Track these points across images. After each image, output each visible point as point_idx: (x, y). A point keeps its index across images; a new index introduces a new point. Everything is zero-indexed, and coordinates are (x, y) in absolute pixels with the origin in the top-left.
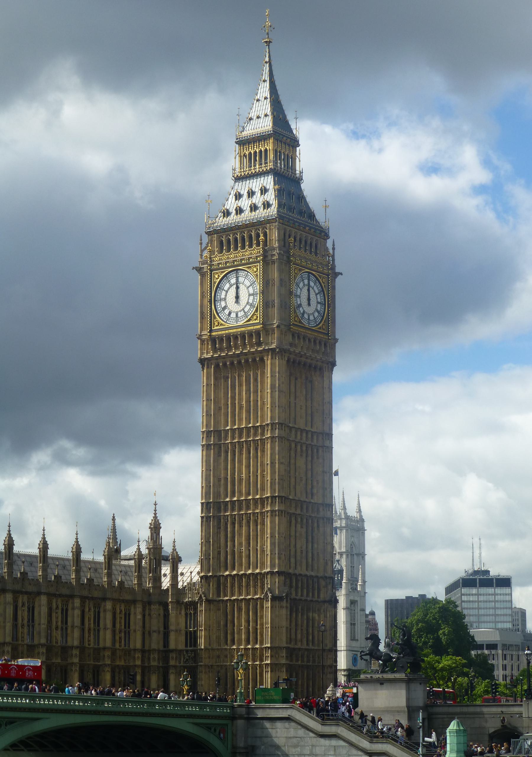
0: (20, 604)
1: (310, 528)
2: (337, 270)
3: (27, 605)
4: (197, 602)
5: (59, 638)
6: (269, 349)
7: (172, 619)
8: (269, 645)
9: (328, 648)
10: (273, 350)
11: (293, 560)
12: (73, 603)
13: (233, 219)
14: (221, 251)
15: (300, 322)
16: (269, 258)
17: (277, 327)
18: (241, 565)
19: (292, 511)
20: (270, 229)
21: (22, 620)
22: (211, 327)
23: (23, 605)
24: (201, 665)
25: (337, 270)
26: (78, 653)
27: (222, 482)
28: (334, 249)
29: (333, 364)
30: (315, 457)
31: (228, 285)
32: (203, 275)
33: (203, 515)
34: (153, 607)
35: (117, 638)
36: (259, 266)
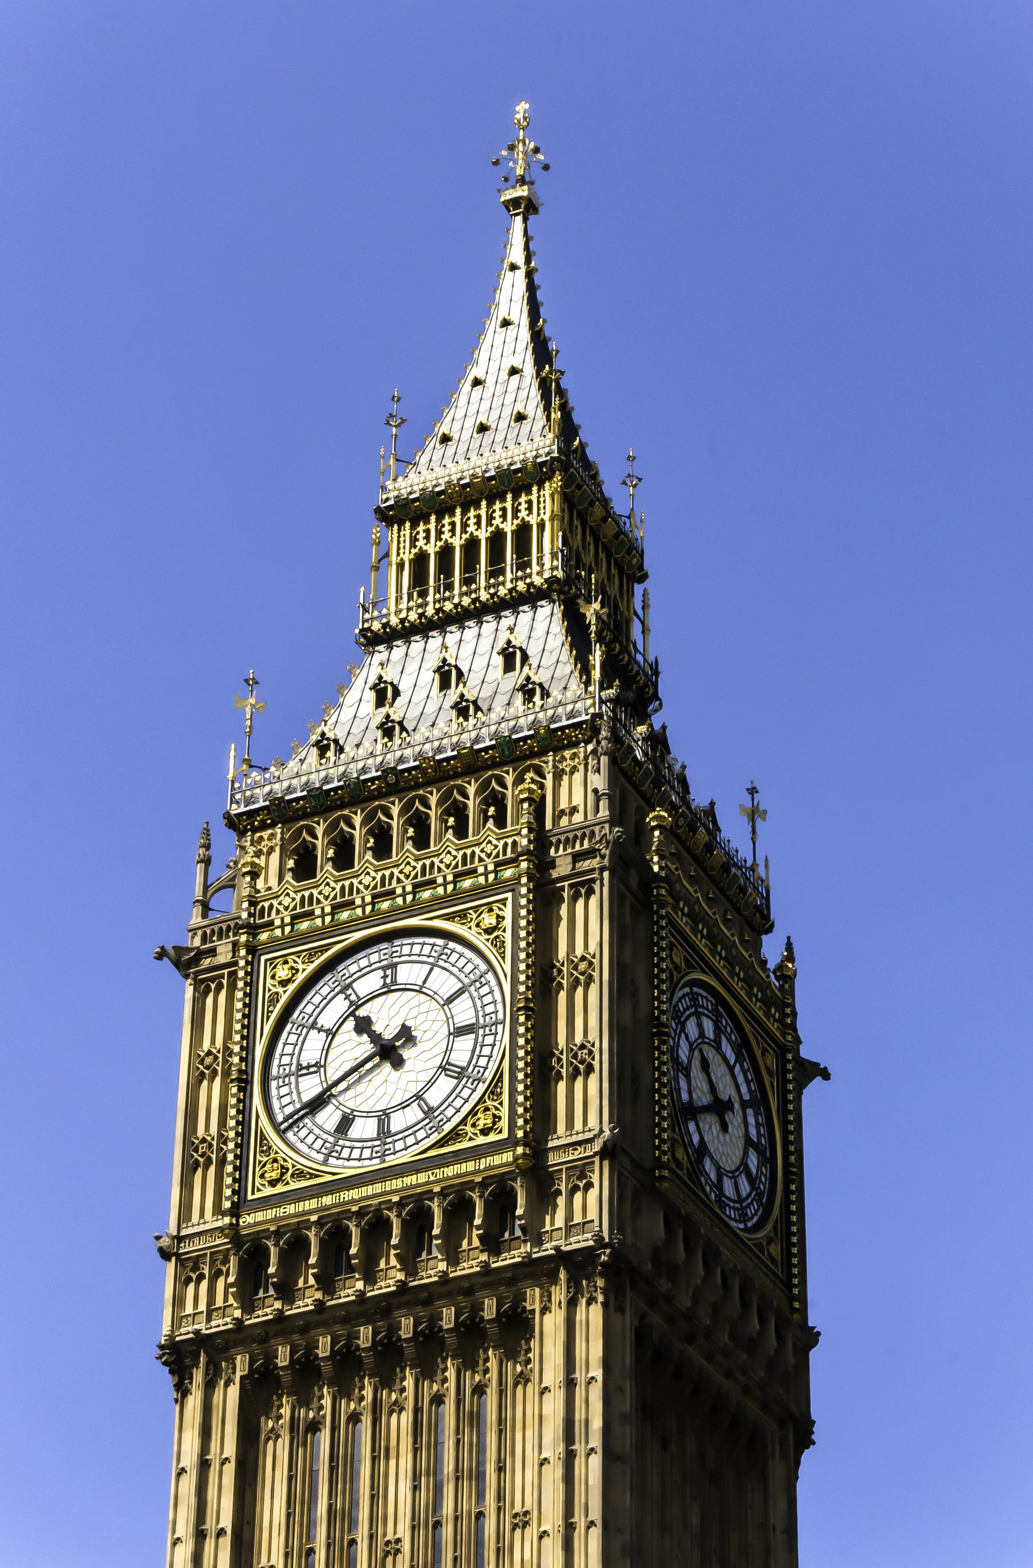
6: (561, 1257)
10: (577, 1265)
17: (603, 1154)
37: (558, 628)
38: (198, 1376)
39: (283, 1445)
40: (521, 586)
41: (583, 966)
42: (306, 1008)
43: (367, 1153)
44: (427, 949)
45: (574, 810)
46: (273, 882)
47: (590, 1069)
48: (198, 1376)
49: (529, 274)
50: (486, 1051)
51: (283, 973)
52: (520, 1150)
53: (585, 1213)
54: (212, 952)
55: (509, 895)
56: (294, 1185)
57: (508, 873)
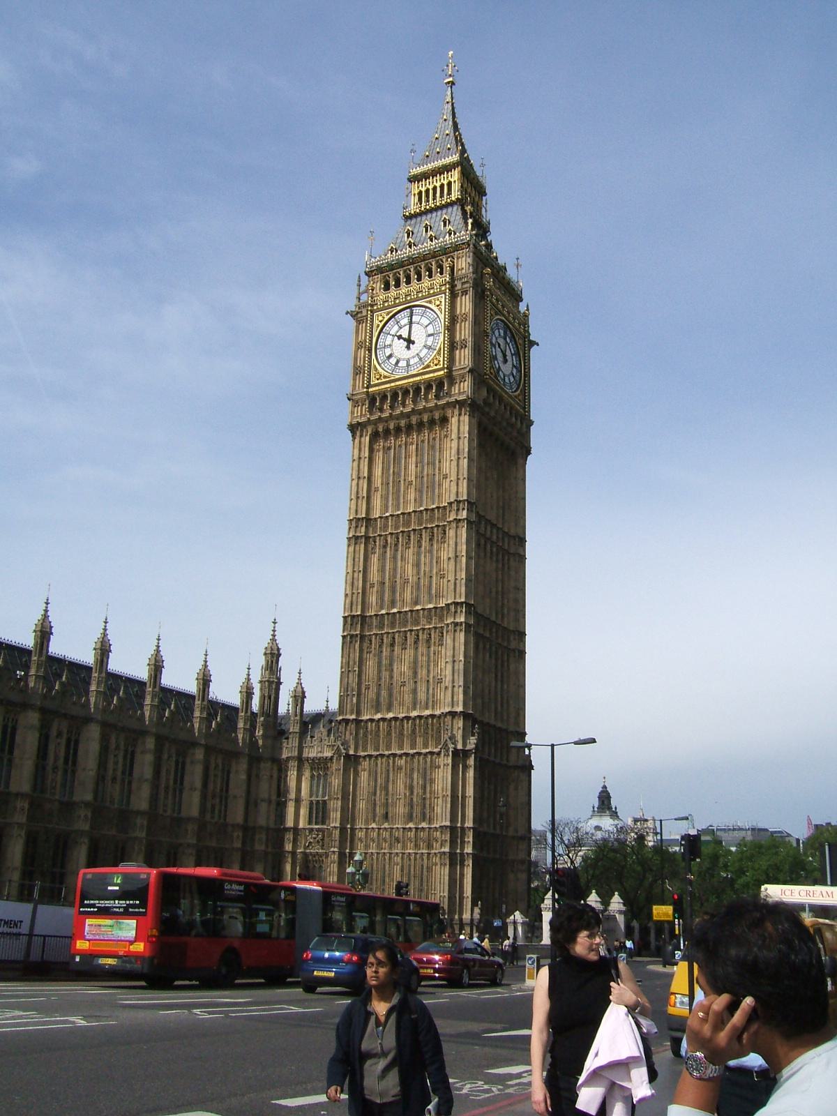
0: (54, 732)
3: (65, 736)
4: (332, 758)
8: (448, 823)
9: (519, 834)
10: (461, 404)
11: (479, 701)
13: (405, 253)
14: (387, 287)
16: (459, 287)
17: (469, 372)
19: (481, 631)
20: (458, 258)
21: (56, 760)
22: (369, 382)
23: (59, 734)
24: (334, 852)
26: (145, 823)
29: (528, 452)
30: (506, 566)
31: (396, 328)
32: (359, 322)
33: (345, 634)
34: (262, 765)
35: (209, 806)
37: (460, 213)
38: (358, 433)
39: (381, 453)
40: (449, 201)
41: (464, 316)
43: (403, 371)
44: (420, 311)
45: (463, 268)
46: (378, 291)
47: (466, 346)
48: (358, 433)
49: (453, 104)
50: (437, 341)
51: (380, 318)
52: (446, 371)
53: (463, 389)
54: (361, 312)
55: (443, 295)
56: (384, 380)
57: (443, 288)
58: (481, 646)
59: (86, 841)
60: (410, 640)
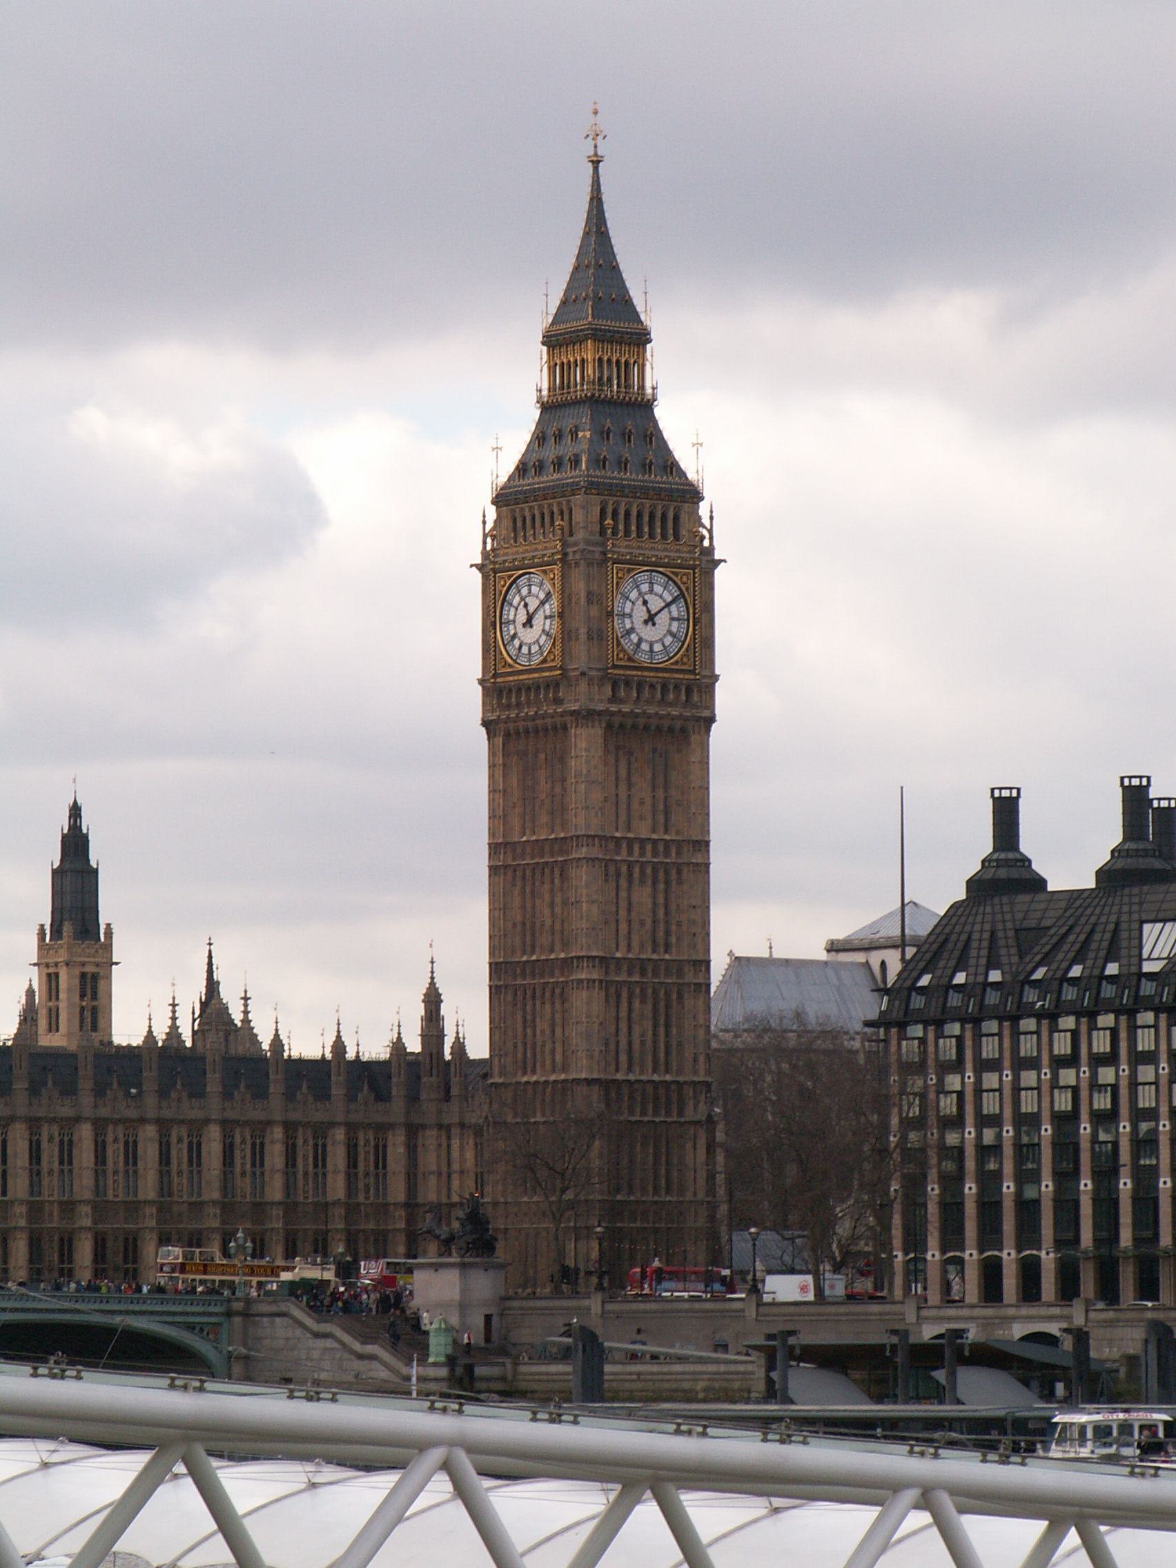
0: (174, 1139)
1: (662, 1004)
2: (717, 557)
3: (186, 1141)
5: (248, 1190)
7: (455, 1154)
11: (623, 1058)
12: (272, 1133)
15: (630, 659)
16: (570, 557)
18: (543, 1066)
21: (179, 1164)
23: (180, 1140)
25: (717, 557)
27: (519, 928)
28: (711, 518)
29: (711, 720)
34: (428, 1133)
35: (361, 1185)
36: (556, 568)
42: (509, 597)
58: (625, 995)
59: (218, 1237)
60: (548, 995)
